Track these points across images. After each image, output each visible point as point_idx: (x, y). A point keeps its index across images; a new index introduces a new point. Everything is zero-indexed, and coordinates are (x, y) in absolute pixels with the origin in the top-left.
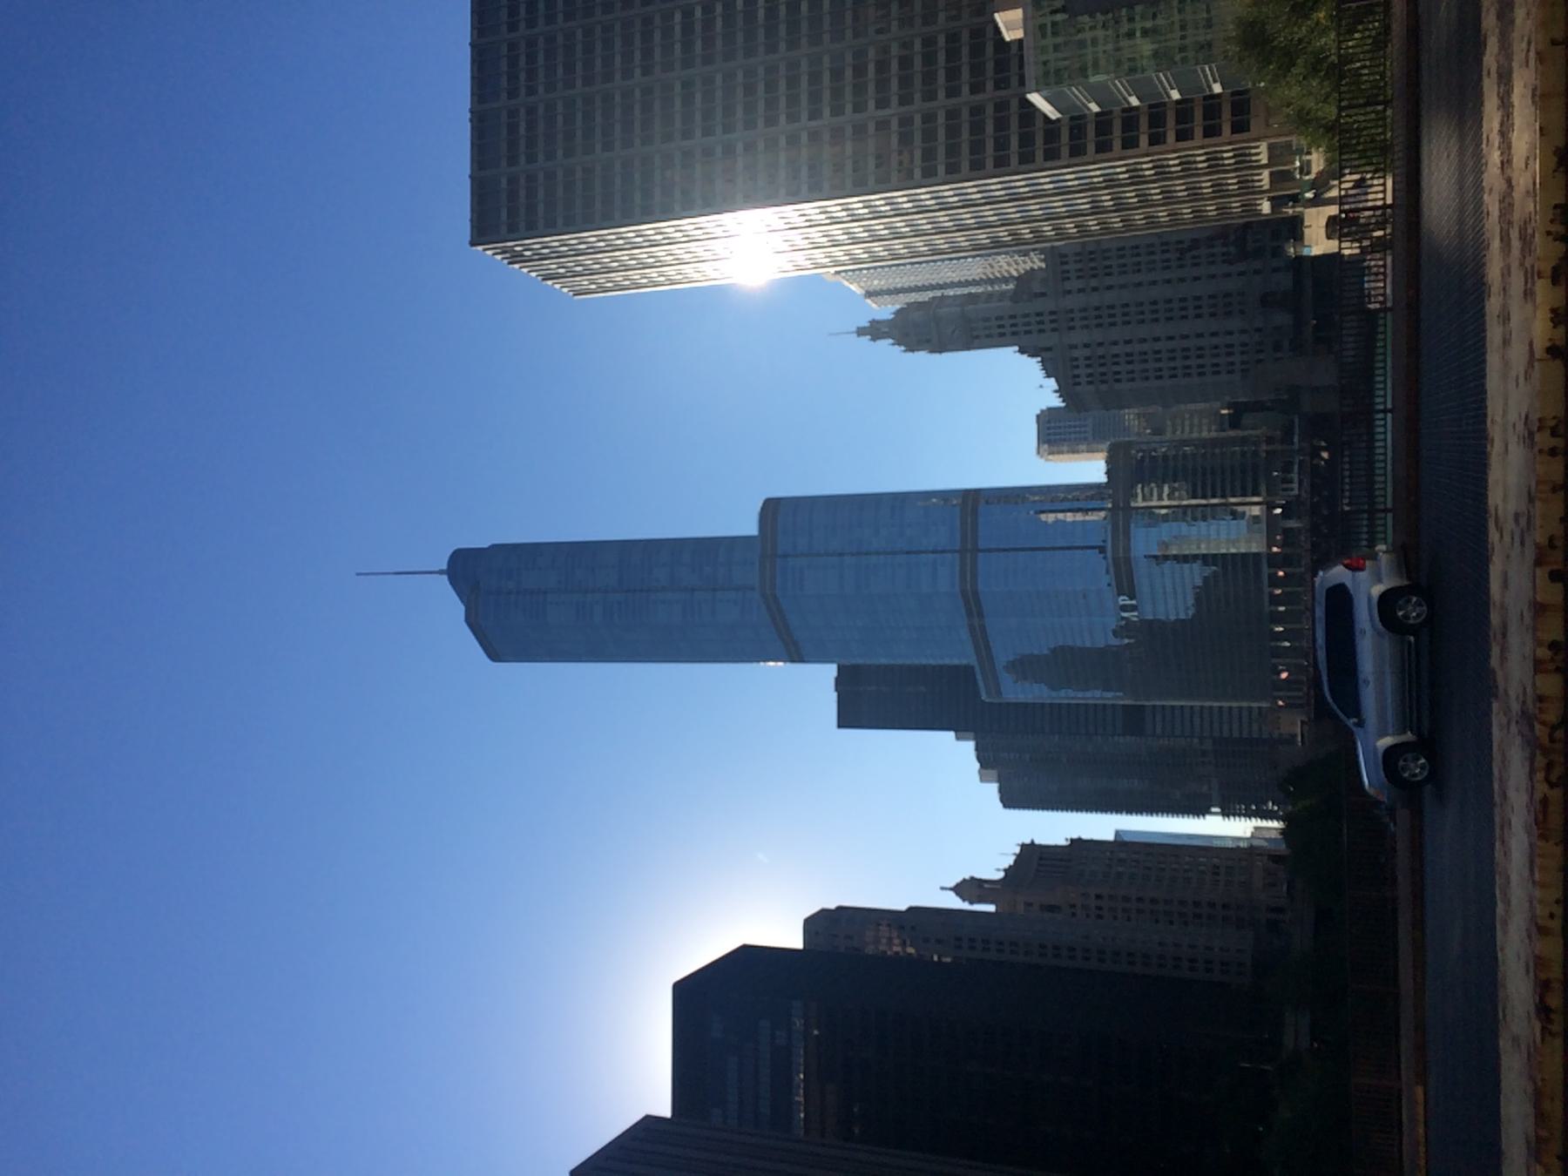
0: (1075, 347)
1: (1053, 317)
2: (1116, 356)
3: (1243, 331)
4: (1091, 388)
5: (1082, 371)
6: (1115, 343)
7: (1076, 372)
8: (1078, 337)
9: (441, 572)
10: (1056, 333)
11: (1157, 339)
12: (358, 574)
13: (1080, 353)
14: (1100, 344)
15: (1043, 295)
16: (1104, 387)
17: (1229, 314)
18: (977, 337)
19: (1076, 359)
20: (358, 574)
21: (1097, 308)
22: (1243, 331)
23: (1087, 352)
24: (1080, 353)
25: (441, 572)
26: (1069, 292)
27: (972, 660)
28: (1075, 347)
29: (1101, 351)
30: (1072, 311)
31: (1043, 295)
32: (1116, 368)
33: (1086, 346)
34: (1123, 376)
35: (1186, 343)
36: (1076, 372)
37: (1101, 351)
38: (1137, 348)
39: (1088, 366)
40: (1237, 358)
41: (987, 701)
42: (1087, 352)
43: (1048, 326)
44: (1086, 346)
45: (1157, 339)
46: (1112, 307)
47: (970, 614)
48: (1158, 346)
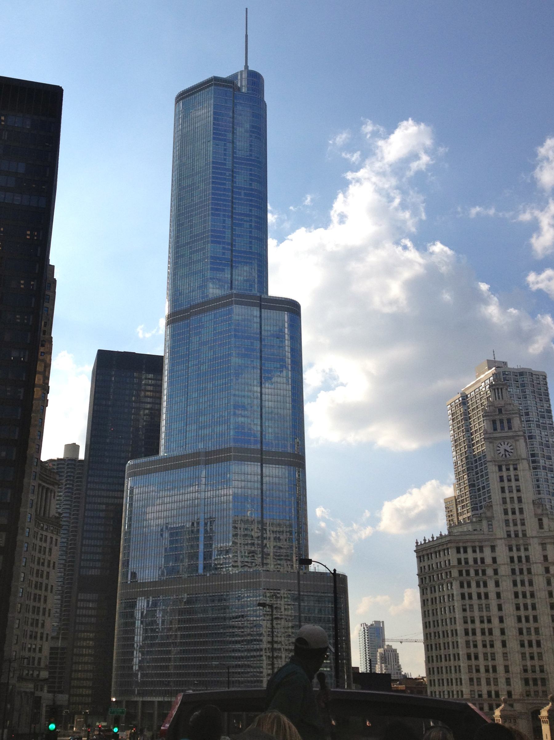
0: (493, 548)
1: (520, 535)
2: (485, 585)
3: (509, 694)
4: (454, 562)
5: (470, 555)
6: (497, 584)
7: (470, 550)
8: (502, 554)
9: (246, 66)
10: (506, 536)
11: (501, 620)
12: (247, 9)
13: (487, 554)
14: (496, 572)
15: (541, 526)
16: (455, 573)
17: (526, 682)
18: (500, 469)
19: (481, 550)
20: (247, 9)
21: (529, 571)
22: (509, 694)
23: (488, 561)
24: (487, 554)
25: (246, 66)
26: (544, 549)
27: (162, 453)
28: (493, 548)
29: (490, 572)
30: (526, 549)
31: (541, 526)
32: (473, 584)
33: (494, 560)
34: (466, 590)
35: (498, 645)
36: (470, 550)
37: (490, 572)
38: (493, 603)
39: (475, 561)
40: (484, 689)
41: (127, 465)
42: (488, 561)
43: (512, 528)
44: (494, 560)
45: (501, 620)
46: (531, 583)
47: (207, 454)
48: (495, 621)
